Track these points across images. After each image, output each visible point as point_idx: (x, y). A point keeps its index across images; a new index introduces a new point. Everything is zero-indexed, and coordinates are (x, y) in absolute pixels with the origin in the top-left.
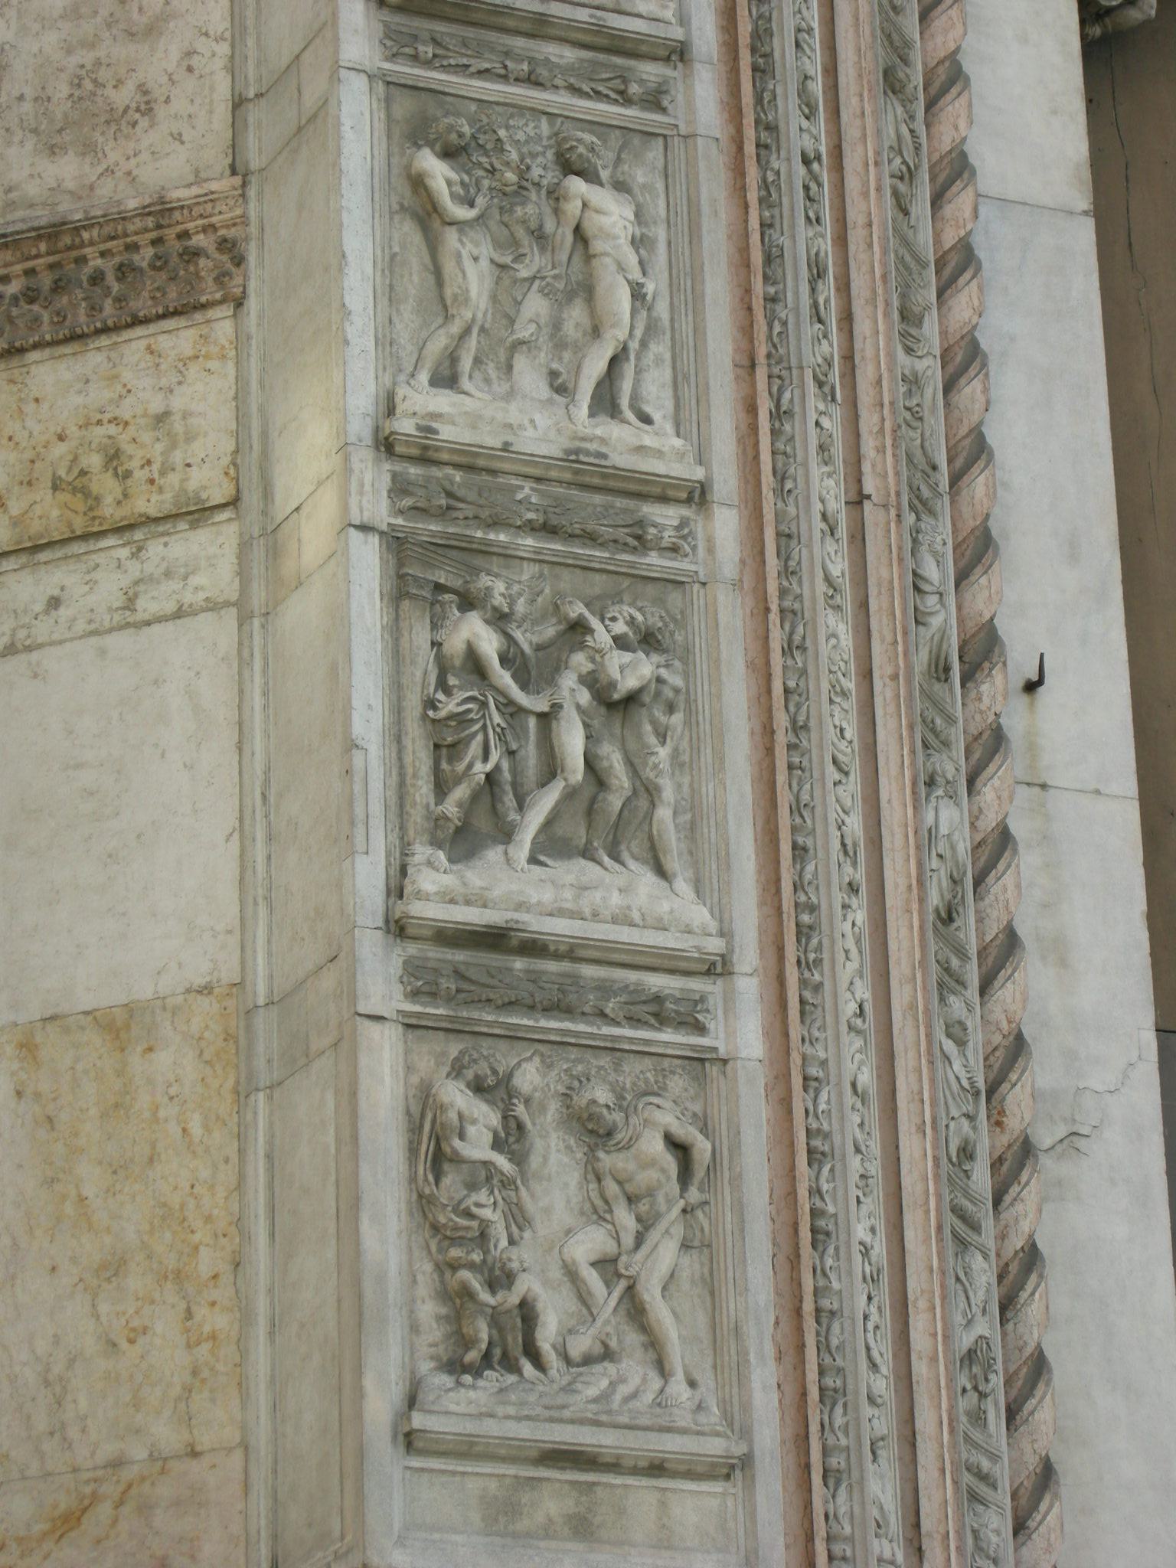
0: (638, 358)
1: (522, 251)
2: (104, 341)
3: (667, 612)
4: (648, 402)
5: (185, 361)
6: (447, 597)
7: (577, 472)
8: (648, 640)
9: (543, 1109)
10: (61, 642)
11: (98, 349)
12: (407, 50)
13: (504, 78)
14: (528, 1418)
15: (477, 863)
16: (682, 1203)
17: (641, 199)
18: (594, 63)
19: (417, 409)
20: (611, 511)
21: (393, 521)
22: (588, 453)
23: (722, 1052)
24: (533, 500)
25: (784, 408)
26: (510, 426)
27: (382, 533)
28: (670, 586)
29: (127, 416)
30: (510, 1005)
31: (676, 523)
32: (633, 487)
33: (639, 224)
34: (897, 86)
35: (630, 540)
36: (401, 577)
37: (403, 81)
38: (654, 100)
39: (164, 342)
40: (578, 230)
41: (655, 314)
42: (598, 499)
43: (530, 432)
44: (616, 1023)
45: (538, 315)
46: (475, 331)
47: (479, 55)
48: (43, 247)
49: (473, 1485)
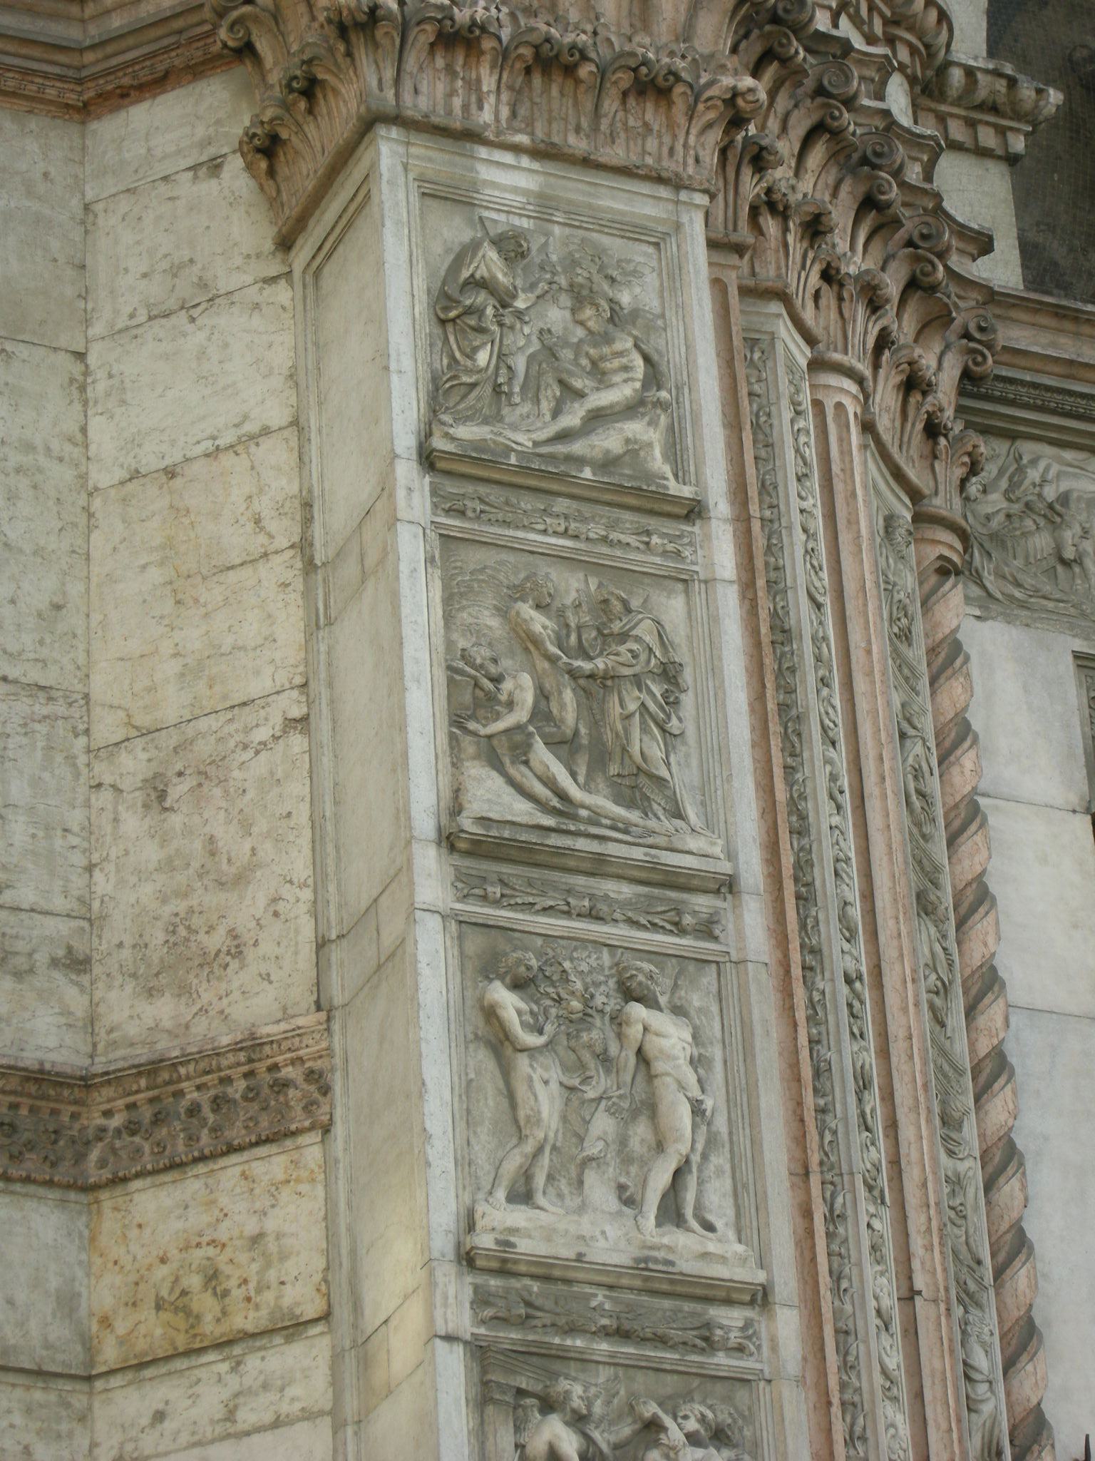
1: (588, 1073)
2: (201, 1168)
3: (736, 1409)
4: (711, 1211)
5: (277, 1185)
6: (529, 1401)
7: (647, 1279)
10: (166, 1454)
11: (196, 1176)
12: (476, 891)
13: (568, 914)
17: (698, 1022)
18: (650, 897)
19: (496, 1224)
20: (680, 1315)
21: (476, 1331)
22: (656, 1261)
24: (607, 1307)
25: (837, 1212)
27: (466, 1343)
28: (738, 1384)
29: (224, 1238)
31: (741, 1324)
32: (699, 1291)
33: (697, 1045)
34: (930, 908)
35: (699, 1342)
36: (485, 1384)
37: (474, 920)
38: (707, 929)
39: (258, 1168)
40: (640, 1052)
41: (714, 1129)
42: (667, 1303)
43: (602, 1243)
45: (605, 1133)
47: (543, 894)
48: (143, 1082)
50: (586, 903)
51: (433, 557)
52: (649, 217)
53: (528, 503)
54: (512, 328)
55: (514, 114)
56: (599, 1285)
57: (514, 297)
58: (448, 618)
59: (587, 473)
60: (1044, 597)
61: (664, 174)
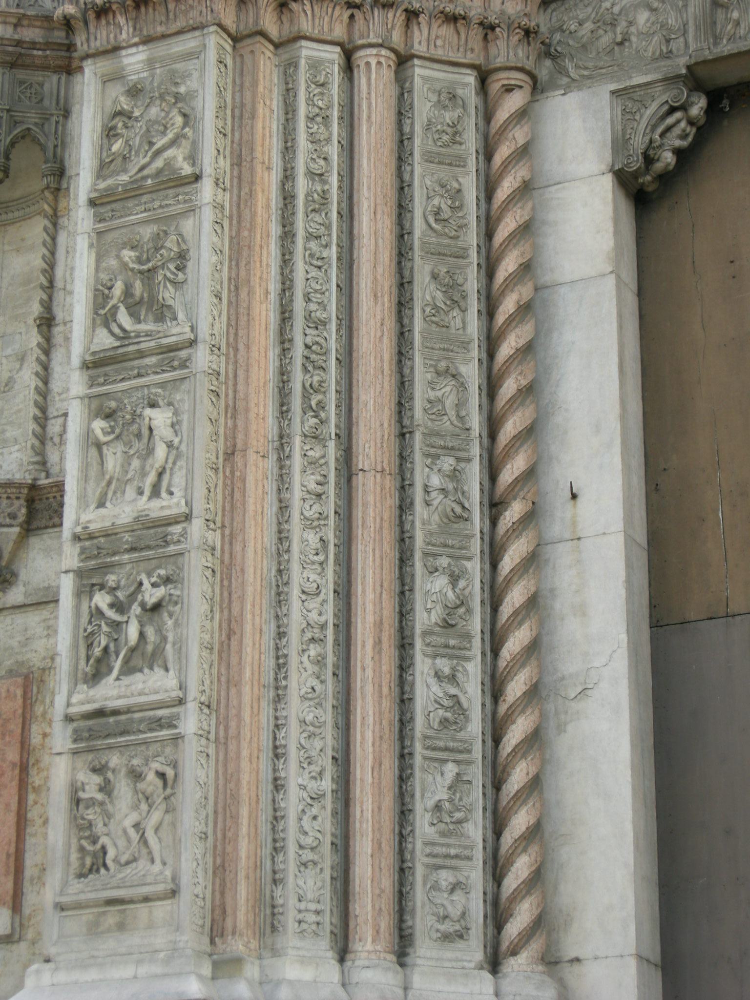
0: (171, 469)
7: (143, 524)
8: (167, 580)
9: (120, 771)
13: (130, 379)
14: (95, 890)
15: (98, 686)
16: (163, 796)
22: (142, 516)
23: (183, 734)
26: (114, 516)
27: (74, 571)
30: (108, 736)
32: (164, 522)
38: (184, 365)
42: (152, 531)
43: (123, 516)
44: (145, 733)
46: (114, 482)
47: (120, 374)
49: (84, 918)
50: (136, 372)
51: (93, 244)
52: (192, 48)
53: (130, 204)
54: (133, 126)
55: (135, 29)
56: (128, 531)
57: (132, 112)
58: (97, 269)
59: (149, 181)
60: (601, 68)
61: (195, 26)
